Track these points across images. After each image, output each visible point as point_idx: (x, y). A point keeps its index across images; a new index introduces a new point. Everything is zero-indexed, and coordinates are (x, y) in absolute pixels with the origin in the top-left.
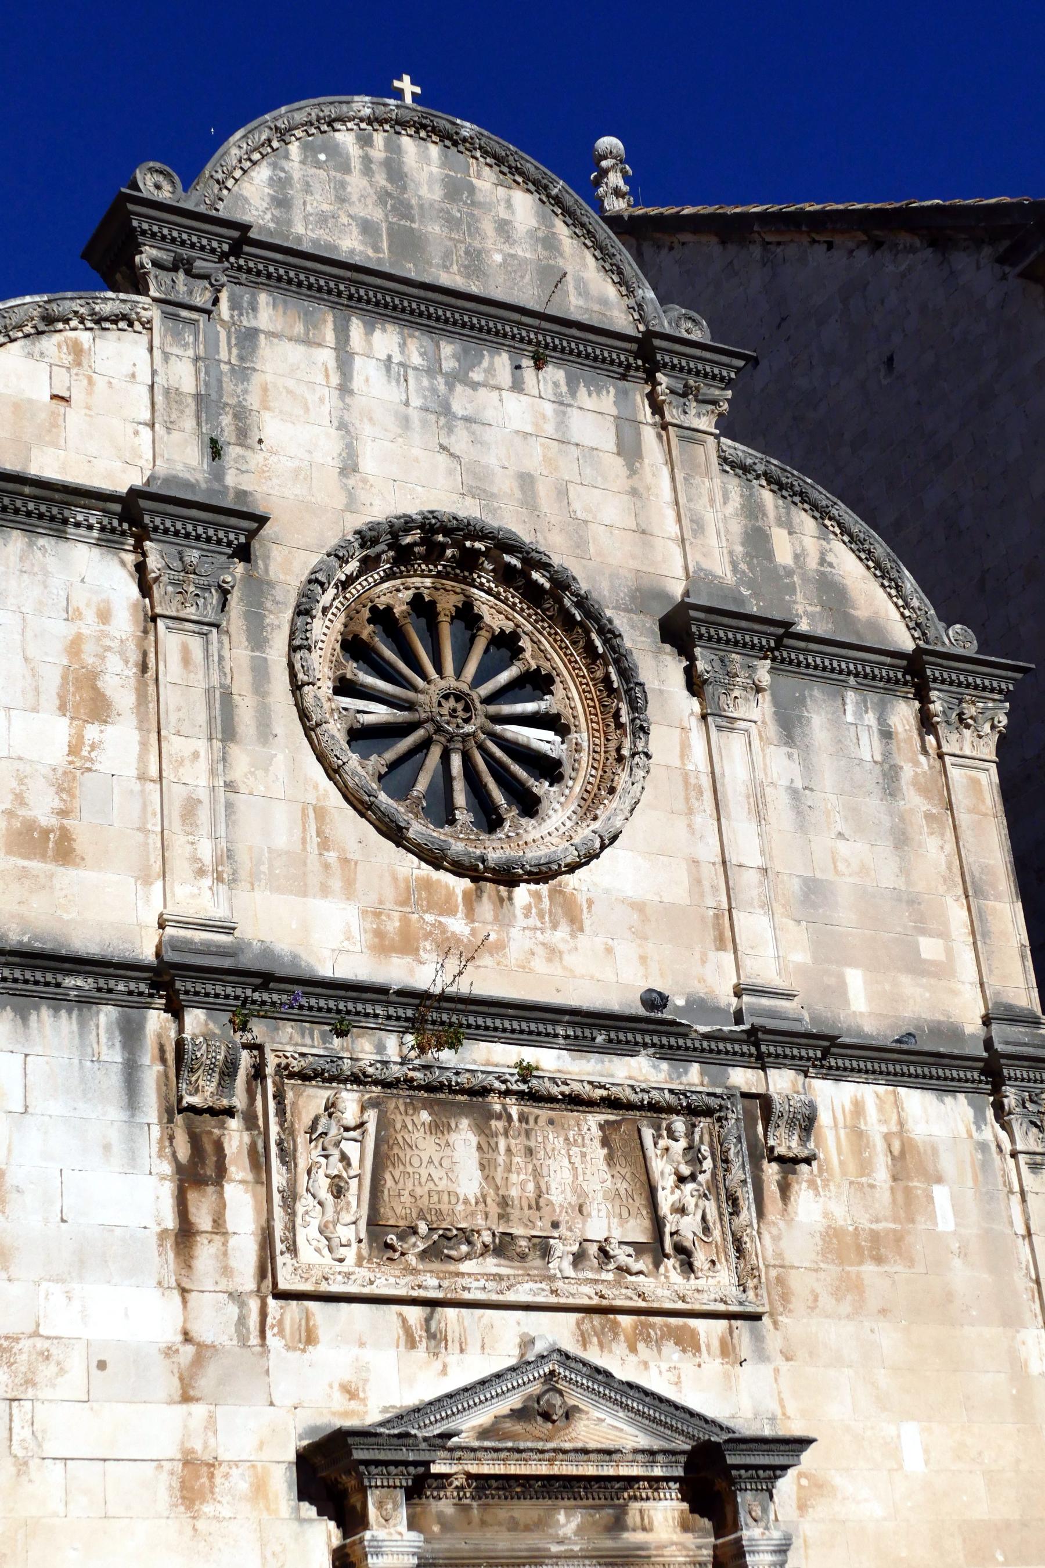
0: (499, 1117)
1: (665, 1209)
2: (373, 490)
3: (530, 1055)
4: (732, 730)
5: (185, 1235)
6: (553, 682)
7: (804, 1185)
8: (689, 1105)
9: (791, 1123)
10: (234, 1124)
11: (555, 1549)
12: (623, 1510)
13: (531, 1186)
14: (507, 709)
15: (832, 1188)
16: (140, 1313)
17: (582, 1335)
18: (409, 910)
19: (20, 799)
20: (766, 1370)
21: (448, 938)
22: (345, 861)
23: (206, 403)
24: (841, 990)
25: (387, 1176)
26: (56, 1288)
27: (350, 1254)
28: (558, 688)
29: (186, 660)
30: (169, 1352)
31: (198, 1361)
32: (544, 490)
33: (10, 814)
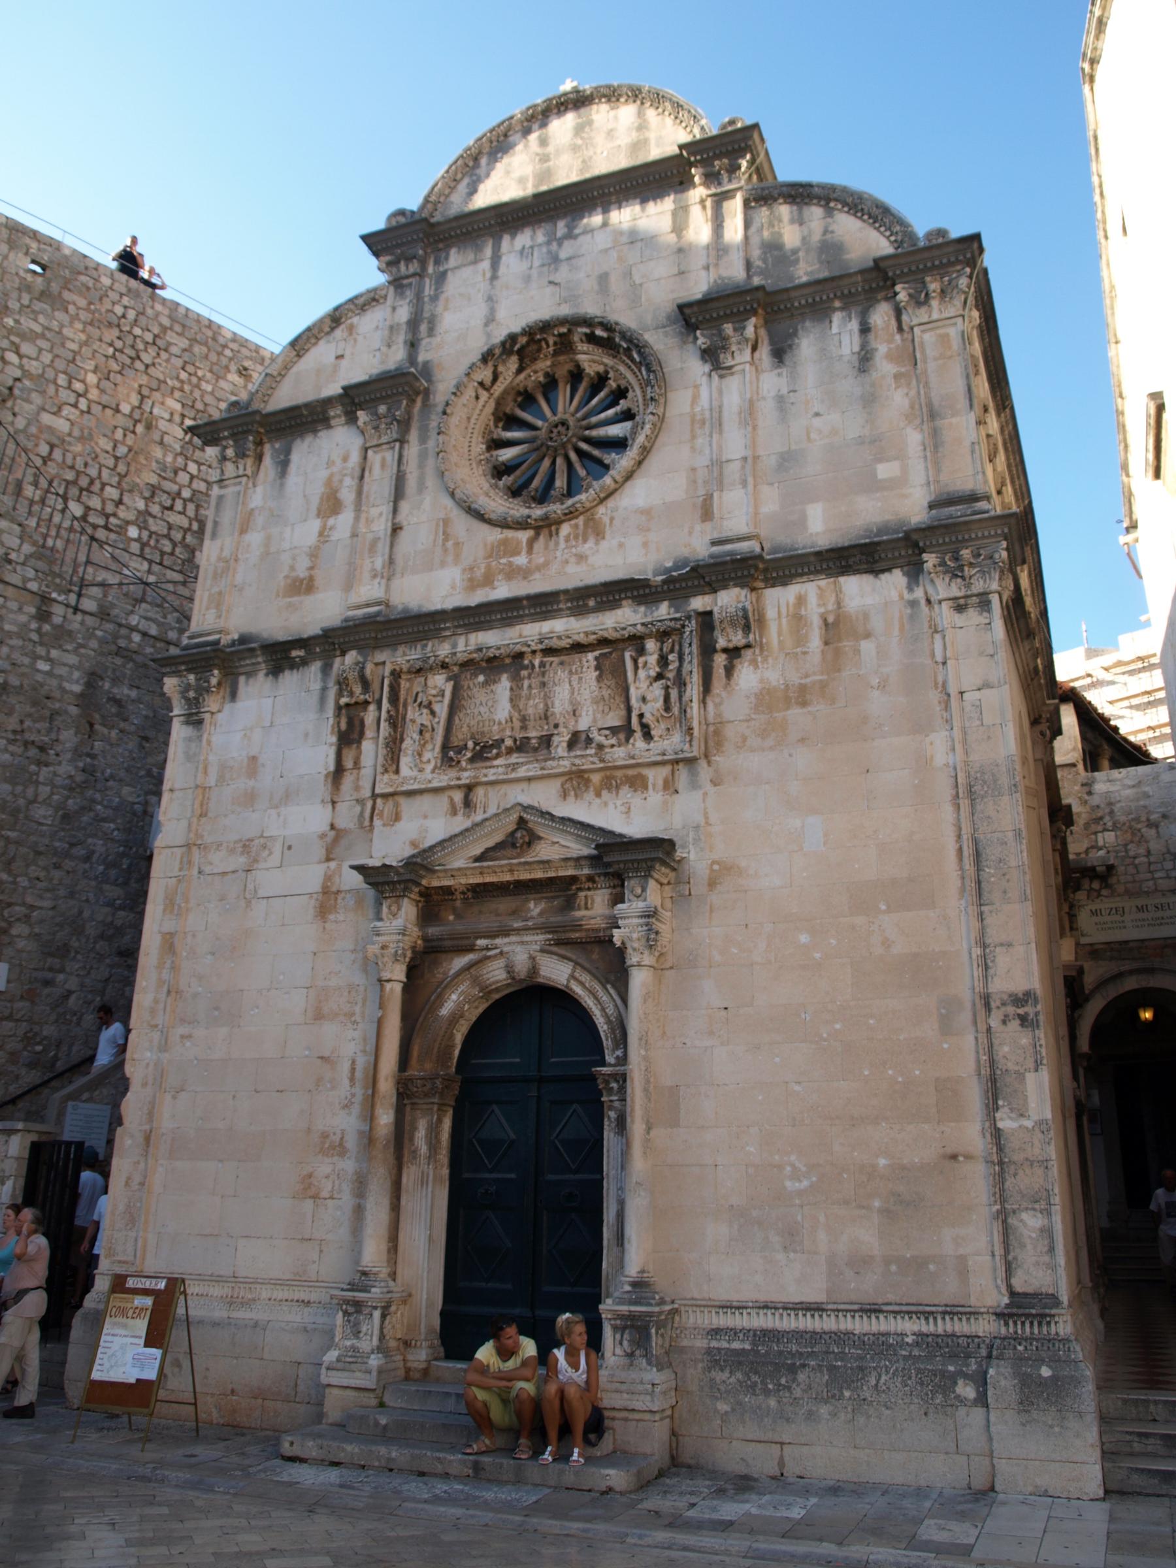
0: (526, 668)
1: (634, 702)
3: (546, 626)
4: (732, 374)
5: (339, 772)
7: (746, 664)
8: (658, 631)
9: (733, 623)
10: (372, 707)
11: (515, 925)
12: (575, 896)
13: (541, 706)
14: (594, 420)
15: (770, 660)
17: (564, 792)
19: (292, 568)
20: (697, 795)
22: (457, 544)
23: (413, 324)
24: (803, 521)
25: (456, 718)
26: (273, 812)
27: (429, 768)
28: (630, 394)
30: (323, 836)
31: (336, 840)
32: (613, 278)
33: (286, 577)
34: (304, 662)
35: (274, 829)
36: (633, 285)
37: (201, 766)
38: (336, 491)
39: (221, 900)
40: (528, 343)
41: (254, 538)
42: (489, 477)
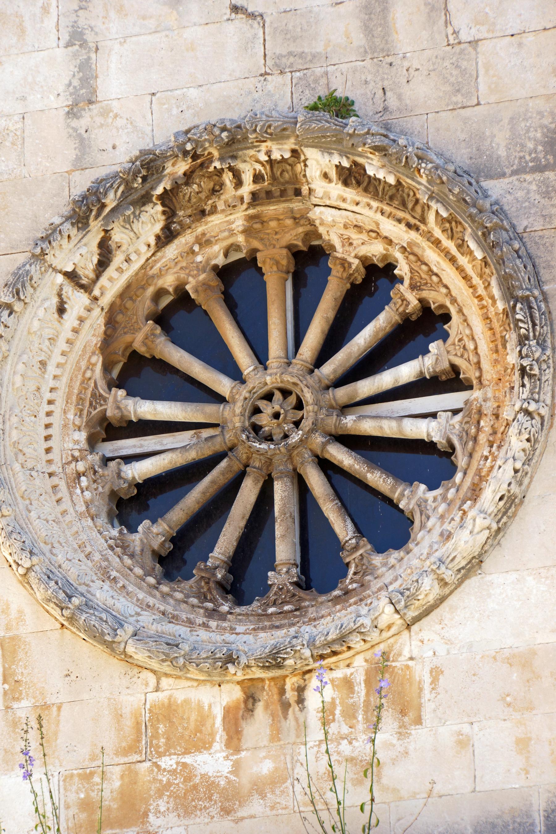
2: (120, 122)
6: (447, 318)
18: (136, 757)
21: (195, 787)
28: (454, 327)
36: (455, 43)
40: (188, 176)
42: (102, 520)
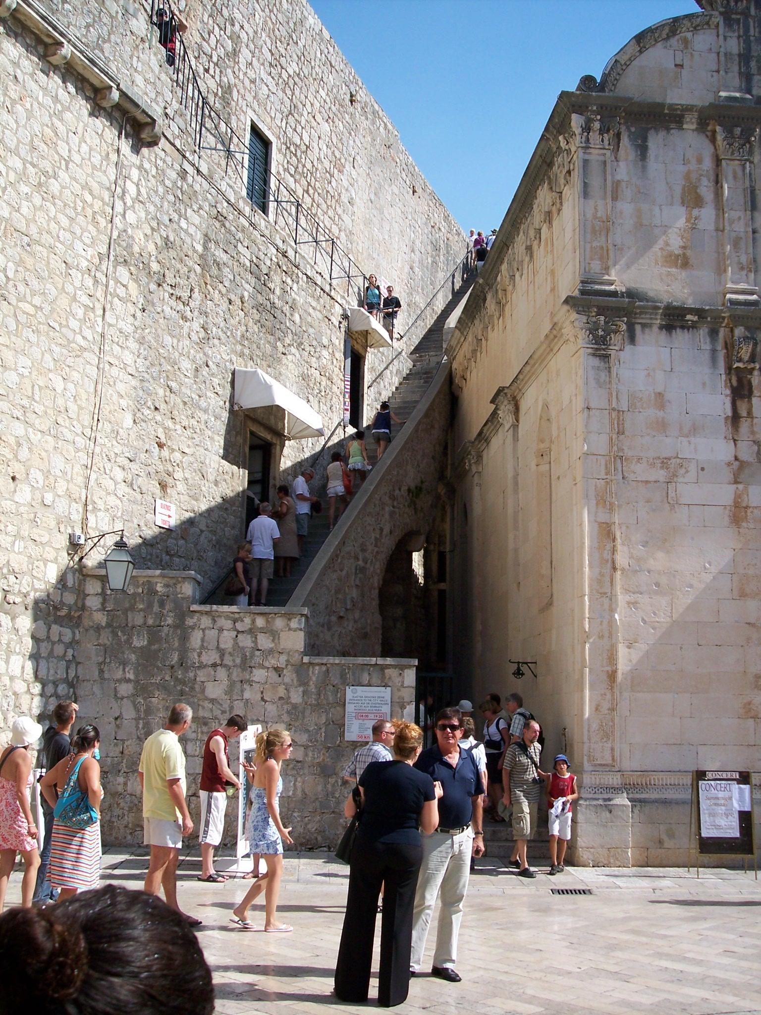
5: (735, 419)
16: (717, 449)
26: (685, 440)
29: (735, 177)
30: (729, 464)
33: (661, 249)
34: (694, 326)
35: (686, 452)
37: (614, 394)
38: (697, 187)
39: (647, 502)
41: (626, 207)
